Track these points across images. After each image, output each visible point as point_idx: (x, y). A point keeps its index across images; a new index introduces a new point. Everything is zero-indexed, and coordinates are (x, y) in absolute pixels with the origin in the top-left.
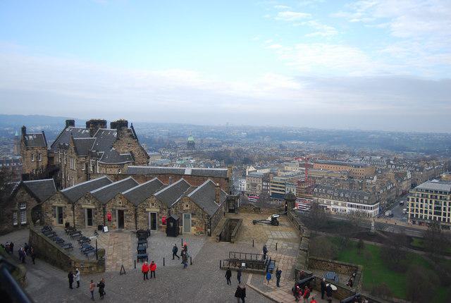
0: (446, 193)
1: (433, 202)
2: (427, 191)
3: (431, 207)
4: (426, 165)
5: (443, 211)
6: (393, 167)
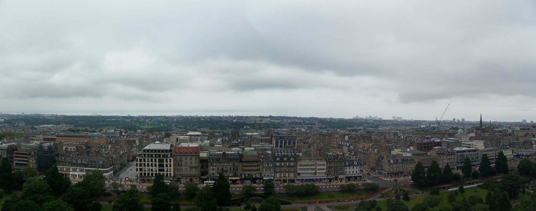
0: (166, 151)
1: (157, 160)
2: (152, 151)
3: (155, 164)
4: (151, 134)
5: (165, 168)
6: (125, 137)
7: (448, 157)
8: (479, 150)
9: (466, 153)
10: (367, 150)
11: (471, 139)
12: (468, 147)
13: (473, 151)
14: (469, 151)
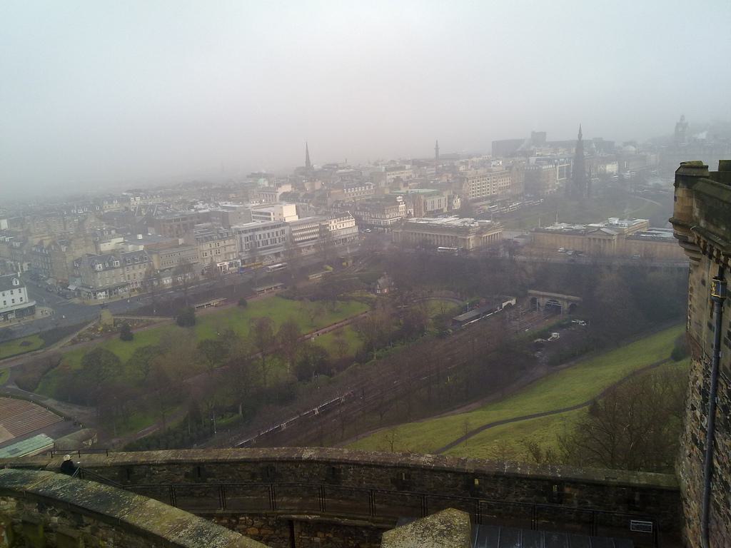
7: (222, 243)
8: (287, 224)
9: (257, 233)
10: (49, 247)
11: (287, 198)
12: (267, 219)
13: (273, 227)
14: (265, 228)
